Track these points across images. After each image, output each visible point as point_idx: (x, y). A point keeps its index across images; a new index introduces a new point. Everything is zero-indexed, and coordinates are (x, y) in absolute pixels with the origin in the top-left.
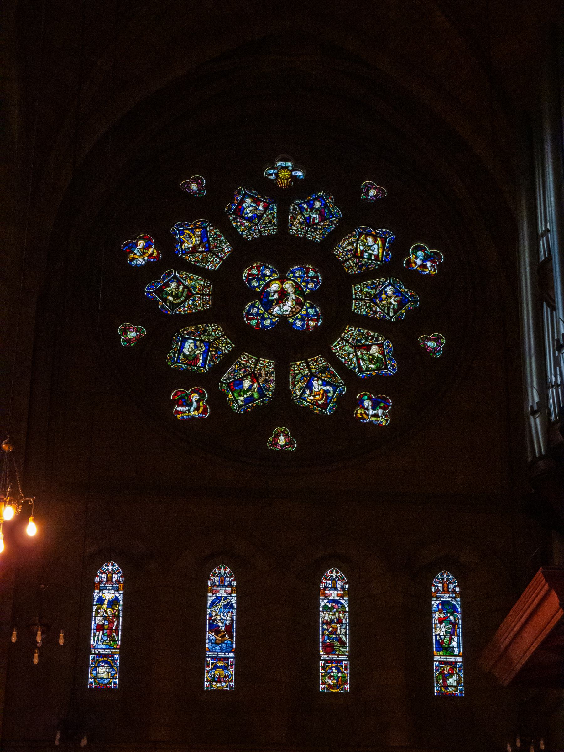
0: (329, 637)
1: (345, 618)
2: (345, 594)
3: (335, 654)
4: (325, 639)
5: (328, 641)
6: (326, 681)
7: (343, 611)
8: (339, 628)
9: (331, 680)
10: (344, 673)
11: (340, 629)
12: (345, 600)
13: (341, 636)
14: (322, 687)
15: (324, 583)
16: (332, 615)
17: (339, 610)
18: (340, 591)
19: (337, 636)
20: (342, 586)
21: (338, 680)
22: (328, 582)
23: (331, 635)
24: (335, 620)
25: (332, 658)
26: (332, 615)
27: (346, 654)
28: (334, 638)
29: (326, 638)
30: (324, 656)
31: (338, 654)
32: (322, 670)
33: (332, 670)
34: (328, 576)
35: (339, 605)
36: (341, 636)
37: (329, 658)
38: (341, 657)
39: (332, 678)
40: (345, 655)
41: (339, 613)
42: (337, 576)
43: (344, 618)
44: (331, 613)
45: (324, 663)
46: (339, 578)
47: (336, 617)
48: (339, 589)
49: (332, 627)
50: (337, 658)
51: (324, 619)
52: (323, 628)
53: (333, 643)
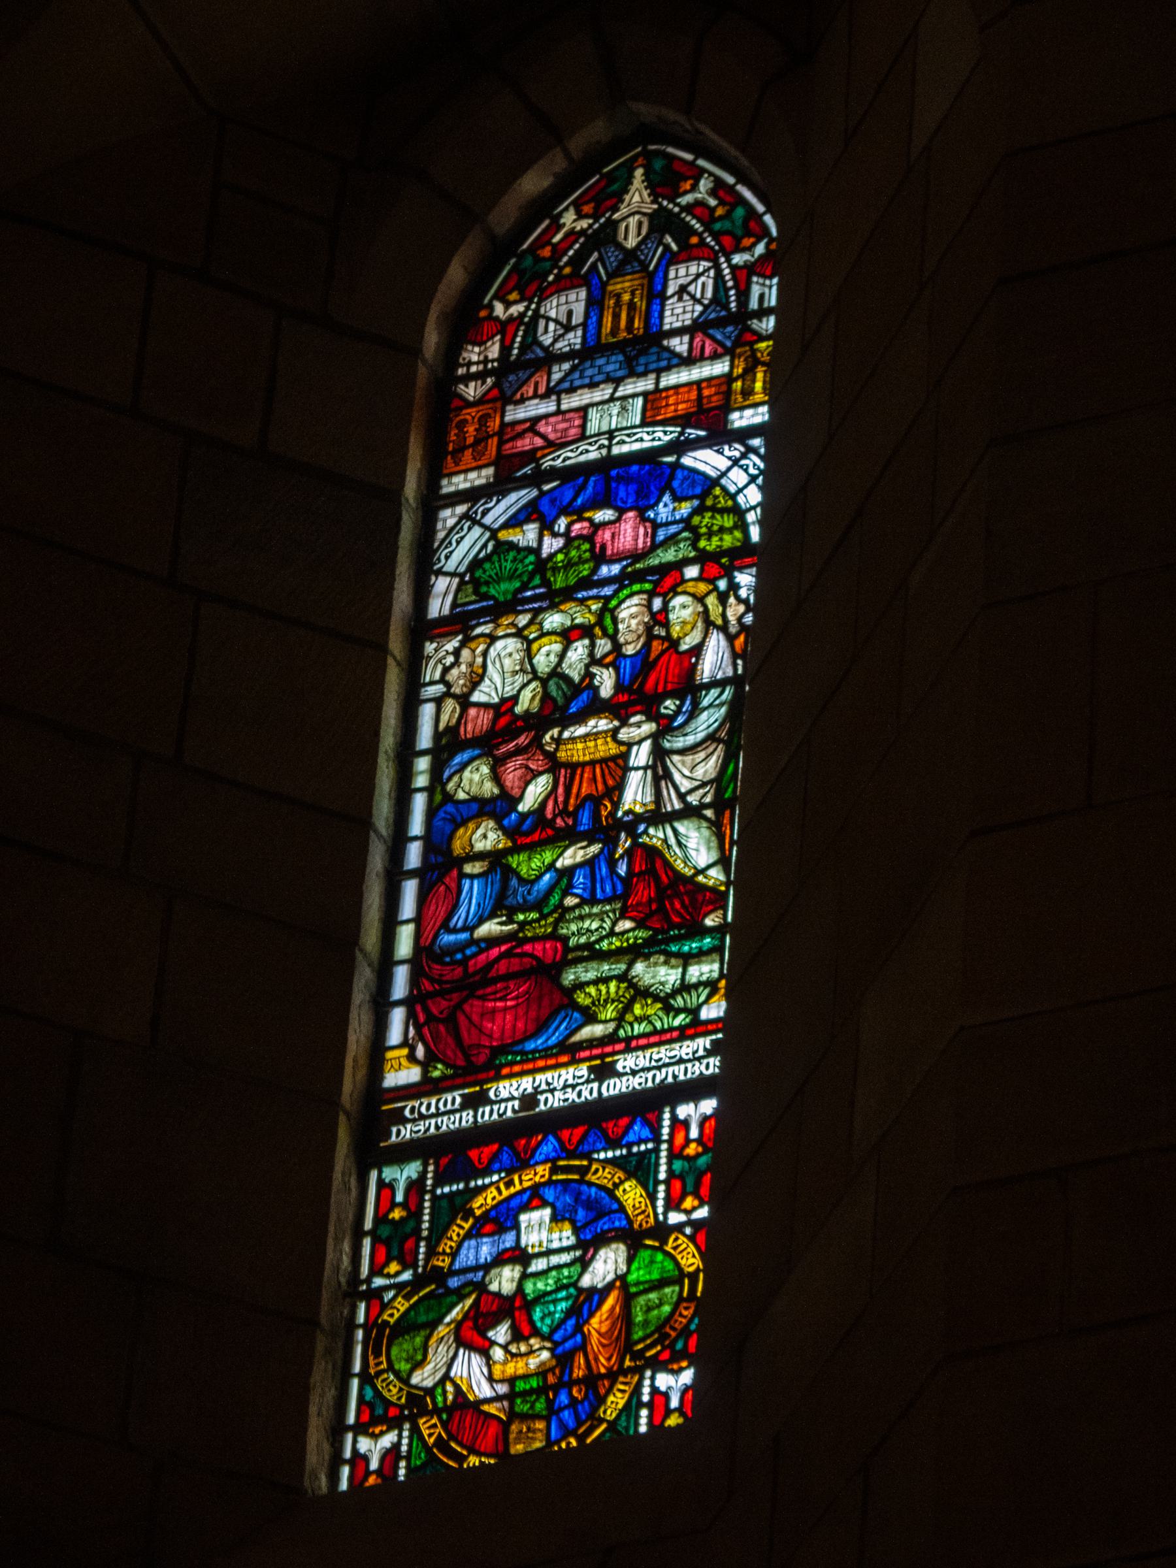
0: (509, 871)
1: (724, 628)
2: (749, 372)
3: (569, 1052)
4: (458, 919)
5: (491, 927)
6: (424, 1378)
7: (703, 558)
8: (641, 755)
9: (484, 1352)
10: (662, 1231)
11: (660, 754)
12: (744, 435)
13: (655, 836)
14: (360, 1460)
15: (505, 327)
16: (568, 636)
17: (669, 555)
18: (689, 361)
19: (611, 843)
20: (719, 300)
21: (578, 1329)
22: (553, 308)
23: (532, 848)
24: (606, 682)
25: (529, 1101)
26: (568, 636)
27: (707, 1013)
28: (570, 871)
29: (473, 895)
30: (426, 1105)
31: (611, 1038)
32: (376, 1270)
33: (508, 1240)
34: (559, 251)
35: (664, 510)
36: (655, 836)
37: (487, 1115)
38: (638, 1059)
39: (501, 1333)
40: (696, 1028)
41: (651, 594)
42: (660, 223)
43: (709, 624)
44: (554, 620)
45: (416, 1187)
46: (683, 233)
47: (617, 647)
48: (679, 345)
49: (554, 765)
50: (589, 1092)
51: (464, 701)
52: (448, 798)
53: (554, 936)
